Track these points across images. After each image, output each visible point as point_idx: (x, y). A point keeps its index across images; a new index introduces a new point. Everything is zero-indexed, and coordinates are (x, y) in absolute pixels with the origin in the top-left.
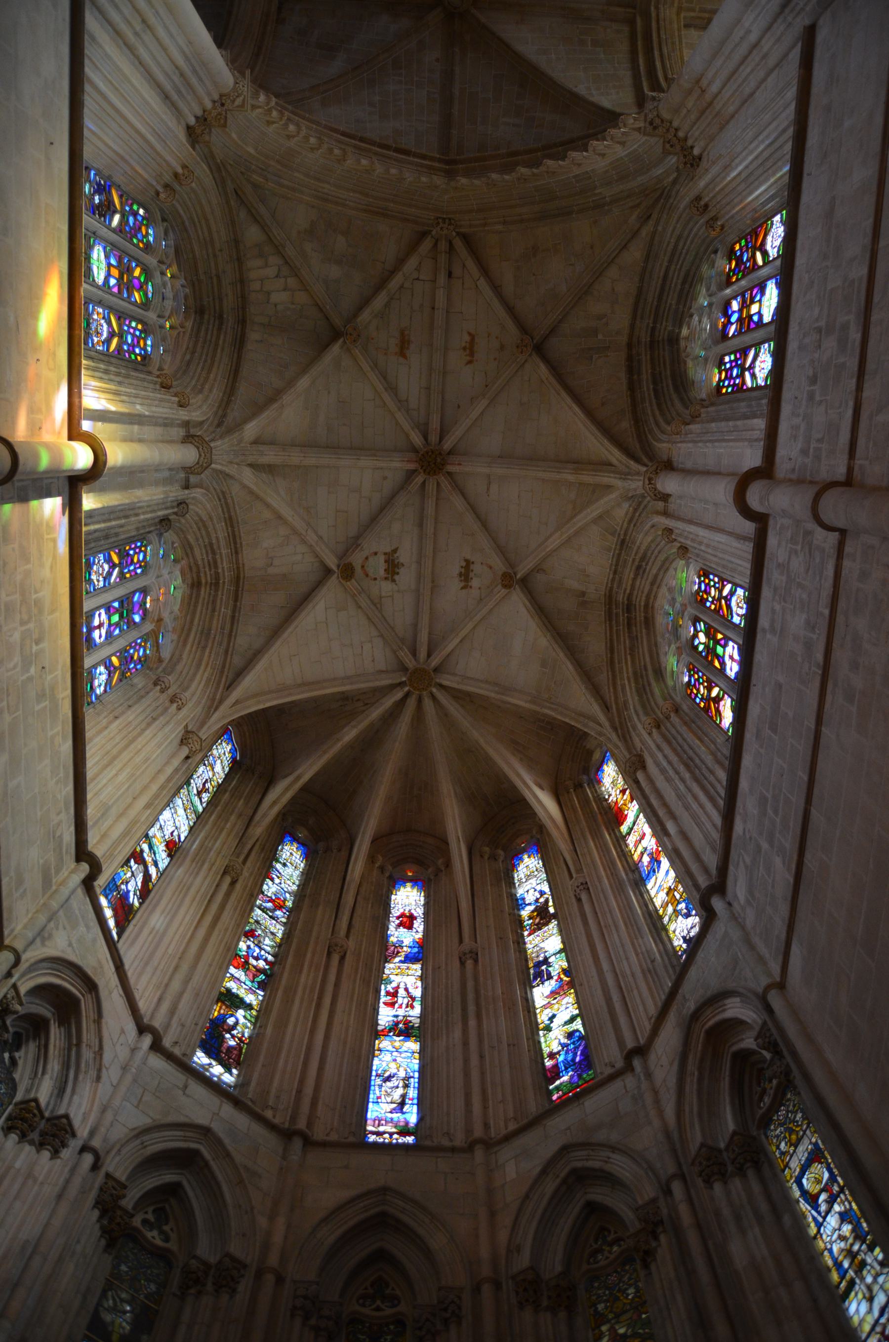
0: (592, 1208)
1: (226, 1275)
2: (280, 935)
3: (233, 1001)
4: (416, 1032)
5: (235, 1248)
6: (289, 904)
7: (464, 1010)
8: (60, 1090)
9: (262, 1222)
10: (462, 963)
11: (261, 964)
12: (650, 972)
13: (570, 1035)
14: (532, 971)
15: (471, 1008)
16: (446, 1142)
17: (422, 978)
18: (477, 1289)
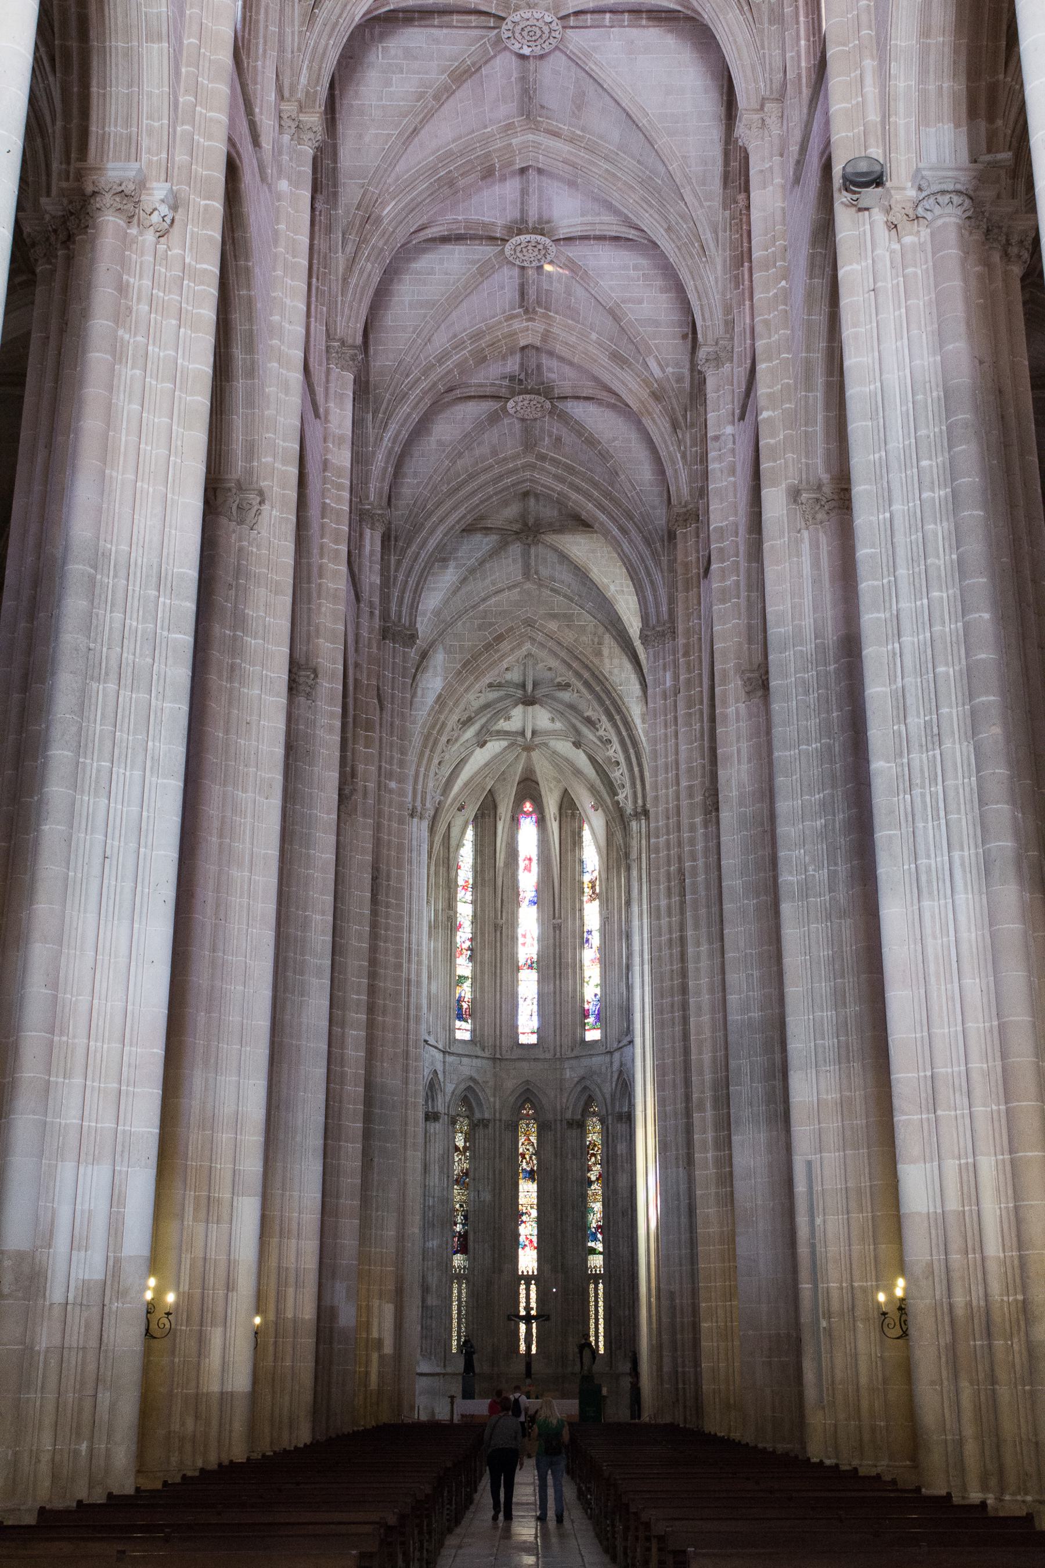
0: (590, 1096)
1: (484, 1123)
2: (470, 913)
3: (462, 979)
4: (535, 965)
5: (487, 1116)
6: (471, 881)
7: (555, 967)
8: (433, 1100)
9: (492, 1099)
10: (555, 932)
11: (468, 944)
12: (621, 1008)
13: (596, 995)
14: (585, 934)
15: (558, 971)
16: (548, 1056)
17: (538, 920)
18: (556, 1120)
